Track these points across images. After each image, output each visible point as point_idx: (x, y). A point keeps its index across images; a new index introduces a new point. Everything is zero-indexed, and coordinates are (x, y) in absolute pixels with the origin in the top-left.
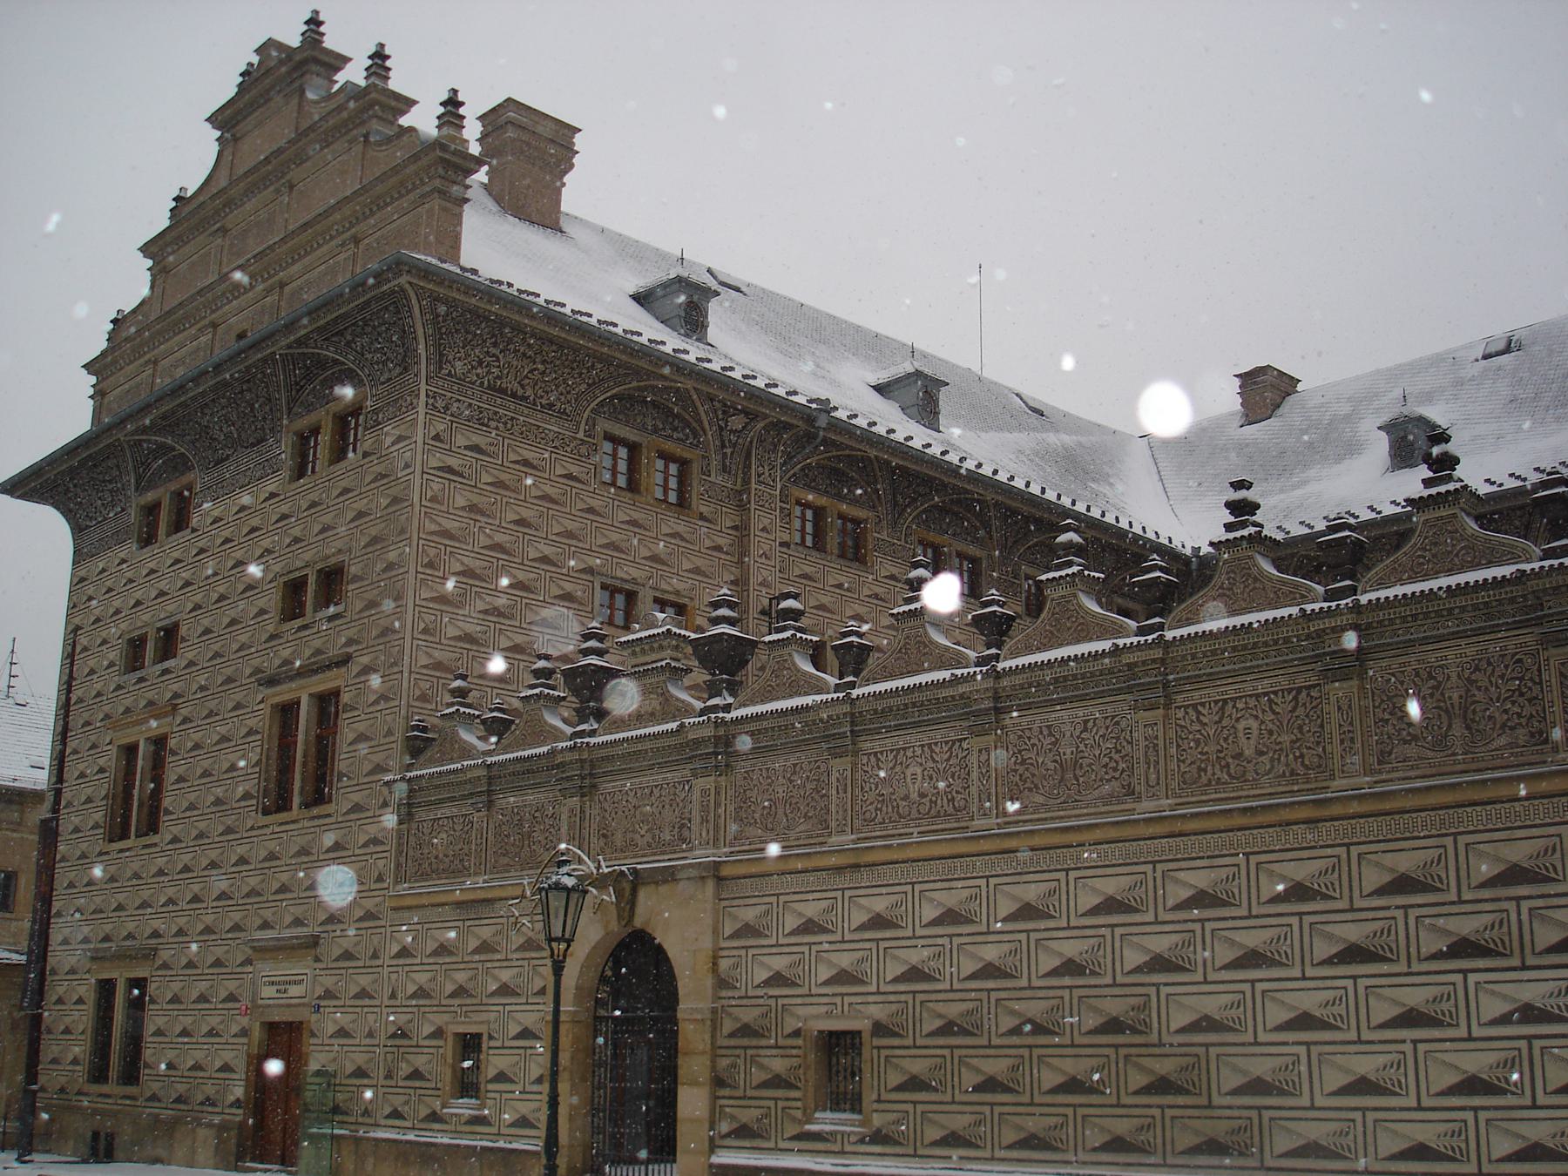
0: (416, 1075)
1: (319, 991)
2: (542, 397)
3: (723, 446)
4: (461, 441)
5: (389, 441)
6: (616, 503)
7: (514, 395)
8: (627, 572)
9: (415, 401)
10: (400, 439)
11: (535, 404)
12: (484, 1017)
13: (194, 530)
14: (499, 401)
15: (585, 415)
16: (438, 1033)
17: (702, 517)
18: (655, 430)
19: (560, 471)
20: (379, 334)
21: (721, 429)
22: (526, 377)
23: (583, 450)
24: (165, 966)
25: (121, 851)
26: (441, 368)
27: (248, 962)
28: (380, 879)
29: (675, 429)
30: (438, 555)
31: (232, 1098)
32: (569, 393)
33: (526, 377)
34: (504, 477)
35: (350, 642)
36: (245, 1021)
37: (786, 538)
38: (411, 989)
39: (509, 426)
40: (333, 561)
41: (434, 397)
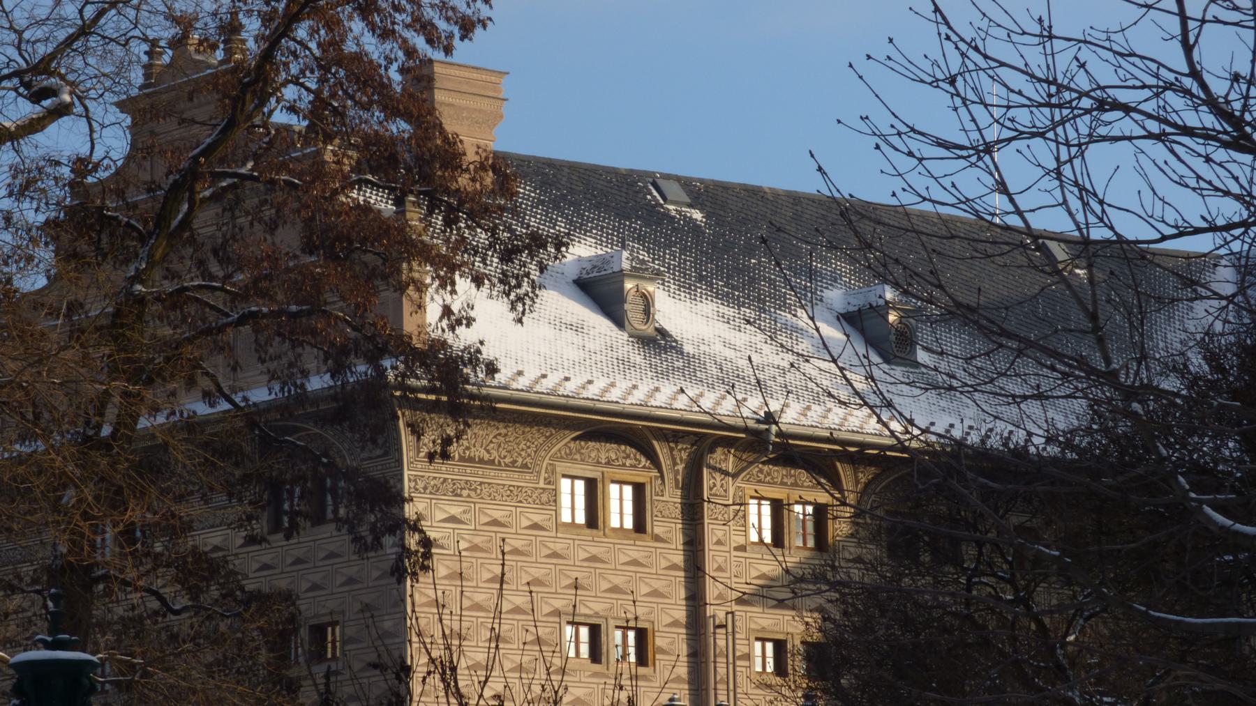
2: (505, 457)
3: (675, 464)
4: (440, 516)
6: (577, 542)
7: (481, 461)
8: (592, 607)
9: (399, 485)
11: (500, 464)
14: (468, 470)
15: (544, 465)
17: (657, 538)
18: (609, 463)
19: (525, 523)
21: (671, 449)
22: (491, 442)
23: (544, 498)
26: (419, 452)
29: (628, 457)
30: (428, 623)
32: (529, 447)
33: (491, 442)
34: (477, 540)
37: (741, 541)
39: (479, 491)
40: (327, 619)
41: (415, 481)
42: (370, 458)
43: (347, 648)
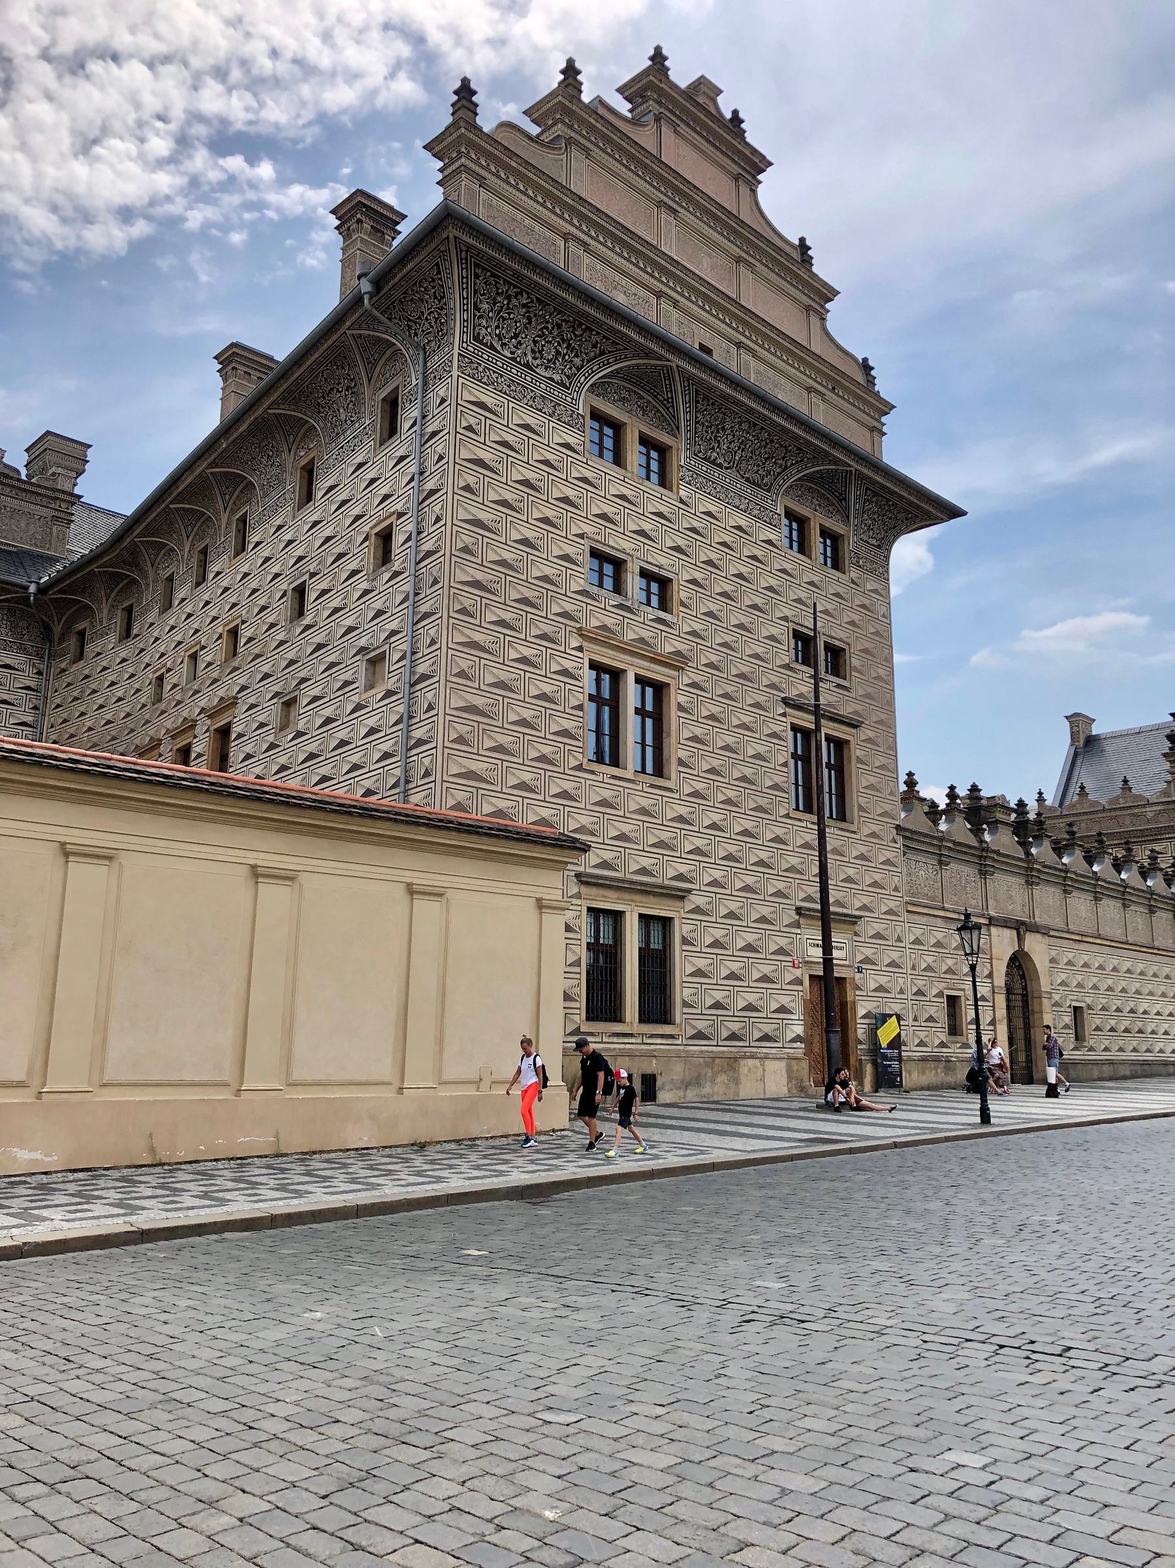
0: (930, 1019)
1: (859, 957)
5: (869, 587)
10: (875, 591)
12: (962, 987)
13: (682, 501)
16: (940, 994)
20: (884, 515)
24: (697, 910)
25: (614, 777)
27: (798, 925)
28: (896, 889)
31: (790, 1035)
35: (861, 716)
36: (798, 972)
38: (924, 965)
42: (866, 541)
43: (853, 673)
